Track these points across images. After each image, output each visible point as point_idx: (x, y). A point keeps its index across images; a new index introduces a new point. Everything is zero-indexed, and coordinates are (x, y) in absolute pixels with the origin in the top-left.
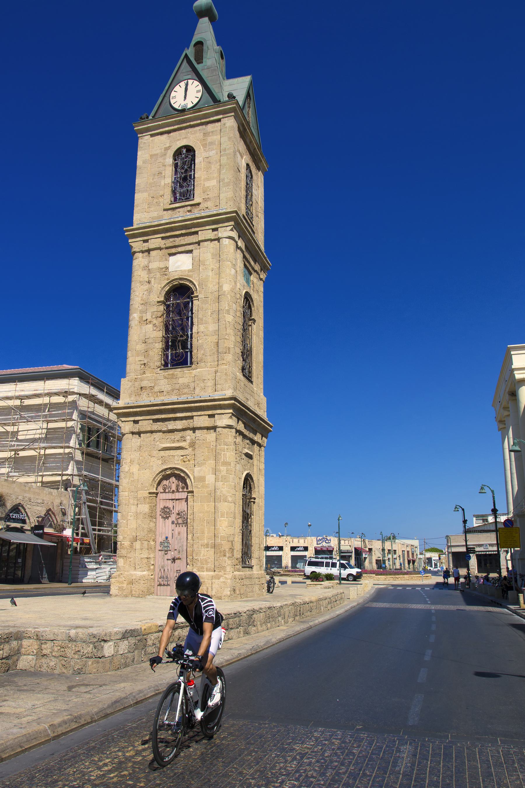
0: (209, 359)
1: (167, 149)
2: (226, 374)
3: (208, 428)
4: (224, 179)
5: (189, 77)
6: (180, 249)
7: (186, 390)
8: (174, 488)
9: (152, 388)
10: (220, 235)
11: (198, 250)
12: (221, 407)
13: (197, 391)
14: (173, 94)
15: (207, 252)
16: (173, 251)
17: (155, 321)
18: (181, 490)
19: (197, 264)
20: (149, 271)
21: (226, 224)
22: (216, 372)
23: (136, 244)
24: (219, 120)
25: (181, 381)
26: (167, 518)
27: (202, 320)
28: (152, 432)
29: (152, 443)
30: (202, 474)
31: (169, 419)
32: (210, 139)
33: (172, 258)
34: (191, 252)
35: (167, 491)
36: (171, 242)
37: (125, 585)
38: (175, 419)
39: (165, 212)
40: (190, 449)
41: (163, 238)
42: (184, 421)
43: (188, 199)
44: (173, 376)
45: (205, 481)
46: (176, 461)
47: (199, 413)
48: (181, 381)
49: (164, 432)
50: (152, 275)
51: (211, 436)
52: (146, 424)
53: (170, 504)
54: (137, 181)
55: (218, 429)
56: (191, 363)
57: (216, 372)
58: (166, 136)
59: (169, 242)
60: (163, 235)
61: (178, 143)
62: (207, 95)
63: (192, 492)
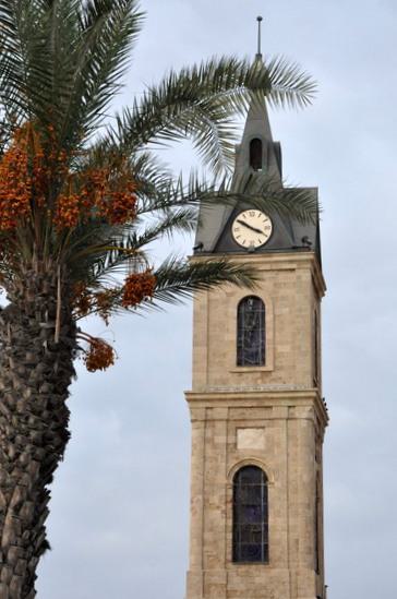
2: (308, 578)
4: (299, 348)
6: (250, 424)
10: (297, 415)
11: (271, 429)
17: (224, 507)
19: (271, 444)
20: (215, 446)
21: (305, 402)
22: (297, 574)
25: (257, 580)
27: (279, 512)
32: (283, 292)
33: (241, 433)
34: (263, 428)
39: (230, 375)
43: (257, 364)
44: (247, 574)
50: (218, 451)
57: (297, 574)
59: (236, 414)
60: (230, 405)
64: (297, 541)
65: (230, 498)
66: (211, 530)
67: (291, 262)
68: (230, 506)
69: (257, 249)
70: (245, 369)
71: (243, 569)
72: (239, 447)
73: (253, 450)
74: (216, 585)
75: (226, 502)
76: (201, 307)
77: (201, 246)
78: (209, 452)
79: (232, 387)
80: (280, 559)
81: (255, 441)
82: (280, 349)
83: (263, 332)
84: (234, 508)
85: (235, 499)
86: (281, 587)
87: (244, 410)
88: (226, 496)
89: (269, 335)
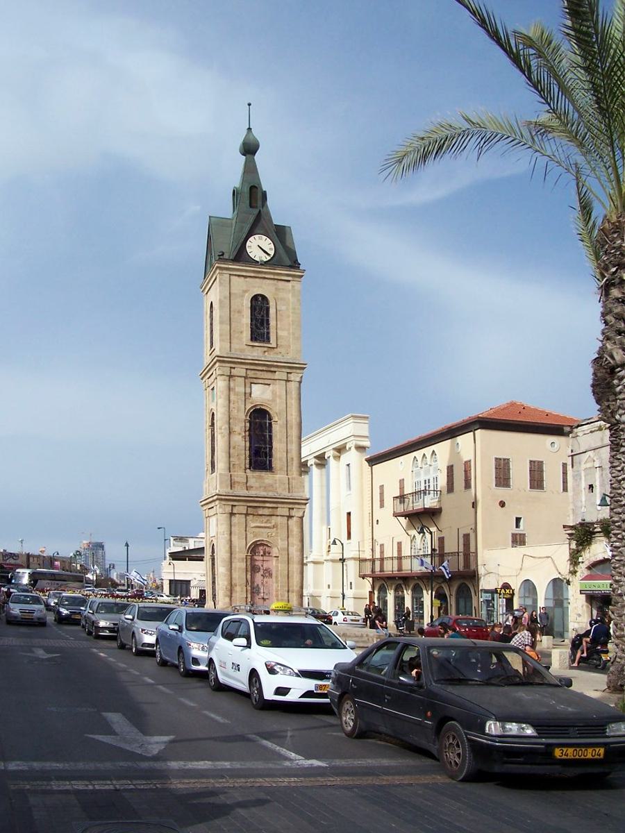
1: (245, 291)
5: (262, 232)
7: (271, 489)
8: (262, 553)
10: (292, 379)
14: (248, 243)
16: (255, 381)
20: (237, 394)
25: (266, 481)
27: (280, 440)
31: (259, 507)
32: (281, 295)
36: (254, 374)
39: (246, 347)
40: (275, 529)
42: (270, 510)
44: (260, 477)
46: (263, 536)
47: (283, 506)
48: (266, 481)
52: (241, 508)
55: (295, 518)
59: (251, 374)
61: (255, 289)
63: (278, 557)
64: (292, 458)
65: (247, 429)
66: (234, 448)
68: (247, 433)
69: (265, 262)
71: (257, 474)
72: (252, 395)
75: (245, 431)
76: (225, 298)
77: (223, 255)
78: (232, 397)
80: (281, 469)
81: (263, 393)
82: (280, 333)
83: (268, 321)
84: (250, 435)
85: (250, 430)
87: (257, 372)
88: (245, 427)
89: (272, 323)
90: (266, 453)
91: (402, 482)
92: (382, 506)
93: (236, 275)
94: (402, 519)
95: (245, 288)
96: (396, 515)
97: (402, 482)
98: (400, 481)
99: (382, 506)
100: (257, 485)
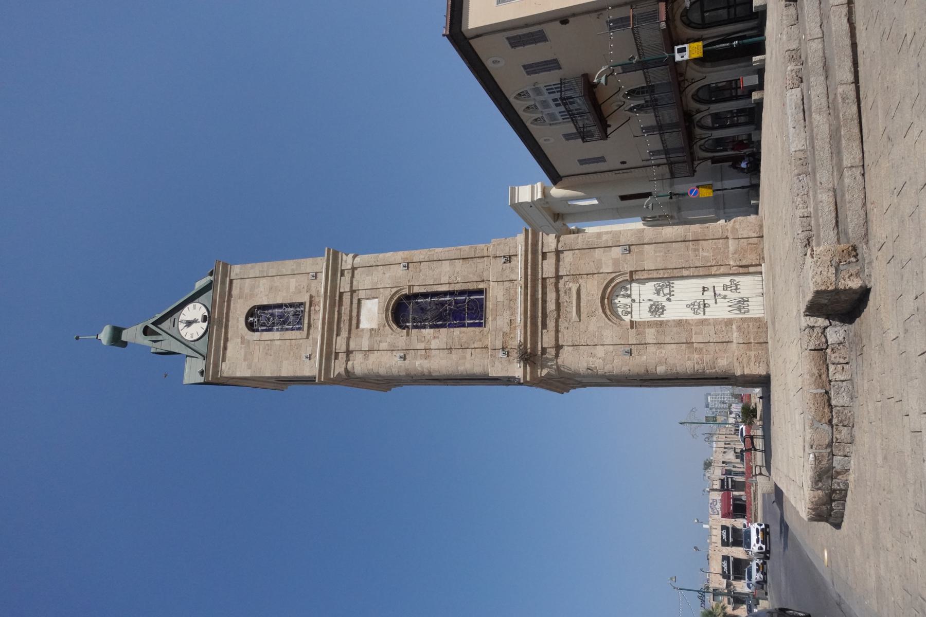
0: (480, 266)
2: (499, 244)
3: (558, 260)
4: (293, 270)
9: (505, 334)
10: (349, 267)
12: (535, 244)
13: (513, 277)
14: (188, 338)
15: (363, 281)
16: (354, 322)
18: (629, 292)
23: (338, 368)
24: (231, 281)
25: (501, 298)
26: (663, 308)
27: (436, 280)
28: (557, 331)
29: (570, 330)
30: (610, 262)
32: (247, 290)
33: (362, 326)
34: (359, 301)
35: (629, 310)
37: (752, 353)
38: (544, 302)
39: (310, 337)
40: (581, 281)
41: (337, 335)
45: (618, 259)
48: (501, 298)
49: (559, 316)
51: (567, 257)
53: (646, 306)
54: (268, 374)
56: (480, 292)
58: (229, 345)
62: (202, 298)
67: (223, 283)
70: (306, 321)
72: (375, 326)
73: (379, 309)
74: (504, 342)
79: (317, 334)
82: (292, 288)
86: (508, 271)
90: (456, 302)
91: (568, 137)
92: (602, 159)
93: (224, 354)
94: (609, 130)
95: (239, 340)
96: (605, 136)
97: (568, 137)
98: (567, 139)
99: (602, 159)
100: (507, 315)
